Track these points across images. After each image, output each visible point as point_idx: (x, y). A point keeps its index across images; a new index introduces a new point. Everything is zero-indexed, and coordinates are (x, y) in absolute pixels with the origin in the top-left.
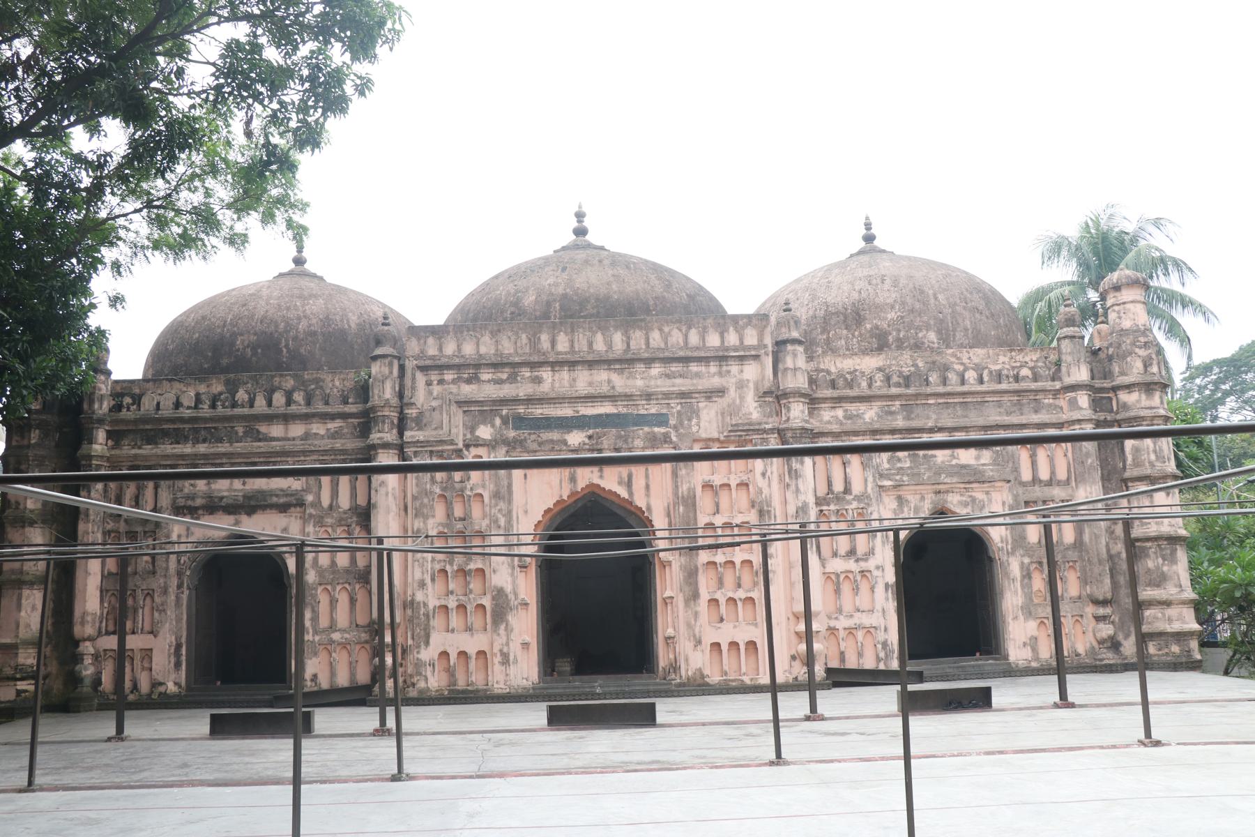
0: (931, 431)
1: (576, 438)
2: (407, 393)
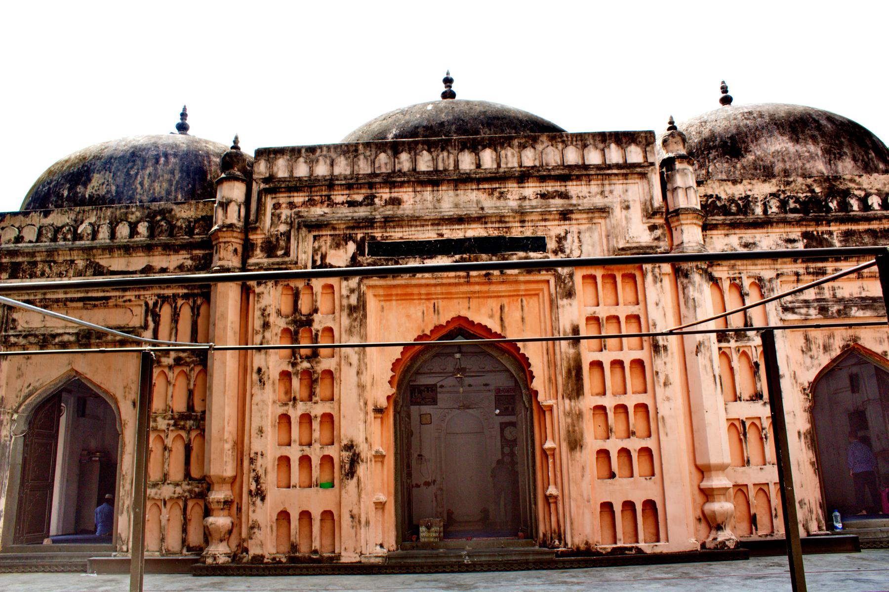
2: (252, 217)
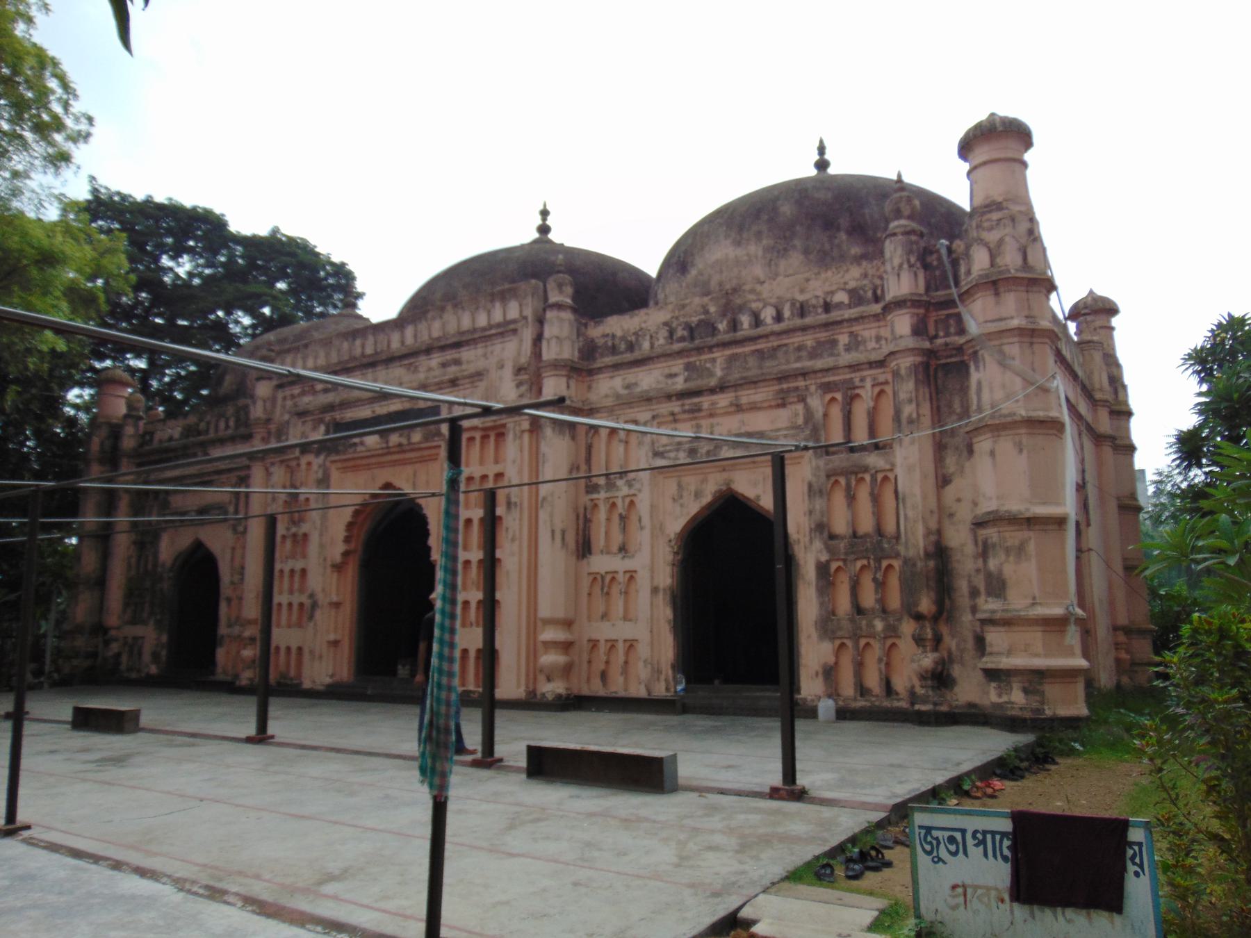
0: (712, 391)
1: (372, 441)
